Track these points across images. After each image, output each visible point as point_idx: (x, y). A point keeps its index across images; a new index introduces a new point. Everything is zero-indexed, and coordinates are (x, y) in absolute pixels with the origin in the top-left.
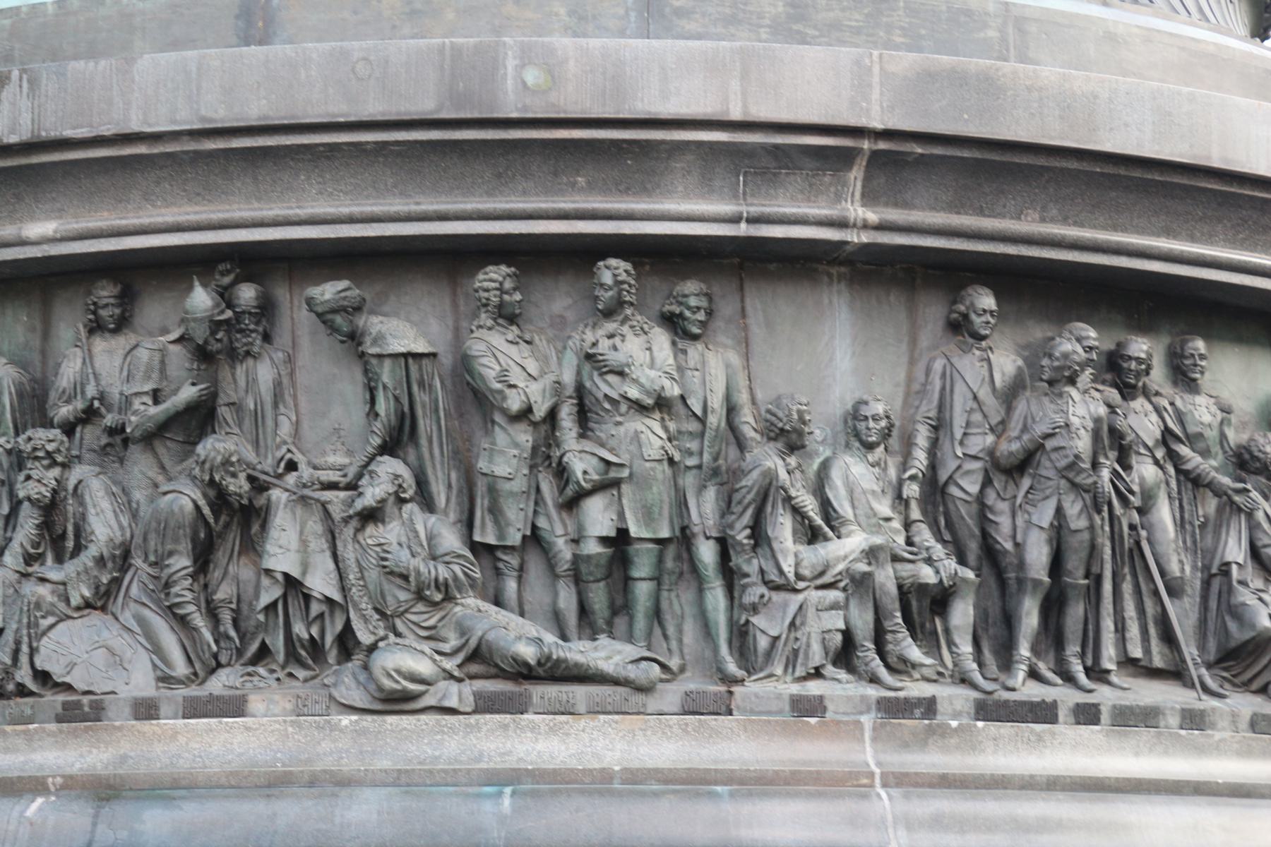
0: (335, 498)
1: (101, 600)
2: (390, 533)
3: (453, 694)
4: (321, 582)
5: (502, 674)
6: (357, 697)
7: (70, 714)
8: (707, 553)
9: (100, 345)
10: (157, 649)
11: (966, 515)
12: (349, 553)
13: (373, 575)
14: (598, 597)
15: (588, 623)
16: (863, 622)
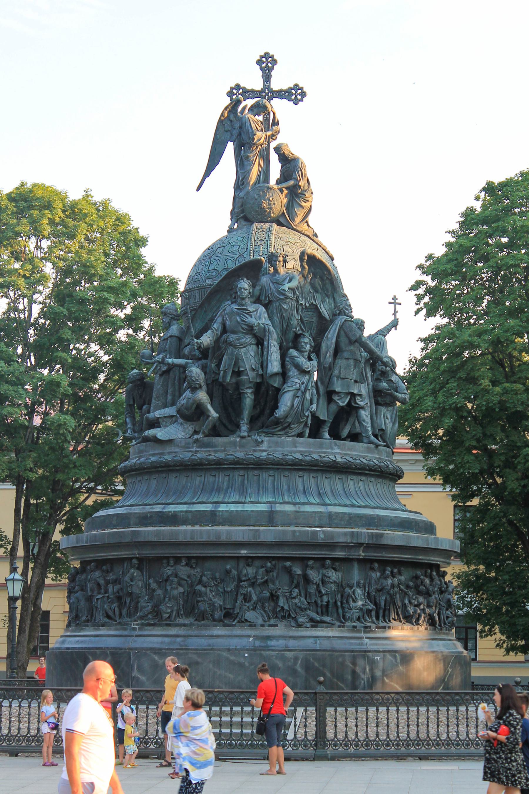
0: (287, 594)
1: (254, 609)
2: (297, 601)
3: (309, 625)
4: (286, 607)
5: (314, 622)
6: (294, 625)
7: (250, 626)
8: (339, 604)
9: (248, 568)
10: (263, 616)
11: (373, 597)
12: (290, 603)
13: (294, 607)
14: (324, 610)
15: (322, 614)
16: (361, 615)
